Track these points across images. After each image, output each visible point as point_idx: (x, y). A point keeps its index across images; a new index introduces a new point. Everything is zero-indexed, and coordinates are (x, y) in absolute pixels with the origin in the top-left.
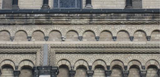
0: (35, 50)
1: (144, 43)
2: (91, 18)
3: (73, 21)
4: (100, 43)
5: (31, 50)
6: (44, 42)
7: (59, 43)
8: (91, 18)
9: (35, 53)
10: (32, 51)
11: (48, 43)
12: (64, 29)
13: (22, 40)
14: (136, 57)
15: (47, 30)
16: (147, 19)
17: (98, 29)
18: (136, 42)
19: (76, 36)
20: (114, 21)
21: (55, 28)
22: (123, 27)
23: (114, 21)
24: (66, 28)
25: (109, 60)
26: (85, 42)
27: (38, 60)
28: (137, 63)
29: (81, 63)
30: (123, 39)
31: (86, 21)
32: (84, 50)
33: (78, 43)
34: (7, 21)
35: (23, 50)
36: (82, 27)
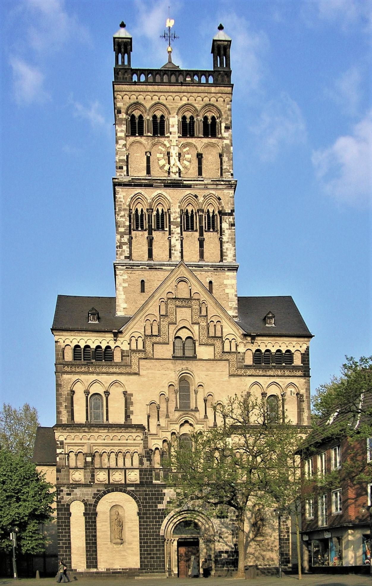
0: (83, 445)
1: (132, 442)
2: (109, 430)
3: (100, 431)
4: (113, 442)
5: (82, 445)
6: (88, 441)
7: (94, 442)
8: (109, 430)
11: (89, 441)
12: (96, 435)
13: (78, 440)
14: (128, 448)
15: (88, 435)
16: (134, 430)
17: (111, 435)
18: (129, 441)
19: (102, 438)
20: (119, 431)
21: (92, 434)
22: (123, 434)
23: (119, 431)
24: (97, 434)
25: (116, 449)
26: (106, 441)
27: (85, 450)
28: (129, 451)
29: (104, 451)
30: (123, 440)
31: (106, 431)
32: (105, 445)
33: (103, 441)
34: (70, 431)
35: (78, 445)
36: (104, 434)
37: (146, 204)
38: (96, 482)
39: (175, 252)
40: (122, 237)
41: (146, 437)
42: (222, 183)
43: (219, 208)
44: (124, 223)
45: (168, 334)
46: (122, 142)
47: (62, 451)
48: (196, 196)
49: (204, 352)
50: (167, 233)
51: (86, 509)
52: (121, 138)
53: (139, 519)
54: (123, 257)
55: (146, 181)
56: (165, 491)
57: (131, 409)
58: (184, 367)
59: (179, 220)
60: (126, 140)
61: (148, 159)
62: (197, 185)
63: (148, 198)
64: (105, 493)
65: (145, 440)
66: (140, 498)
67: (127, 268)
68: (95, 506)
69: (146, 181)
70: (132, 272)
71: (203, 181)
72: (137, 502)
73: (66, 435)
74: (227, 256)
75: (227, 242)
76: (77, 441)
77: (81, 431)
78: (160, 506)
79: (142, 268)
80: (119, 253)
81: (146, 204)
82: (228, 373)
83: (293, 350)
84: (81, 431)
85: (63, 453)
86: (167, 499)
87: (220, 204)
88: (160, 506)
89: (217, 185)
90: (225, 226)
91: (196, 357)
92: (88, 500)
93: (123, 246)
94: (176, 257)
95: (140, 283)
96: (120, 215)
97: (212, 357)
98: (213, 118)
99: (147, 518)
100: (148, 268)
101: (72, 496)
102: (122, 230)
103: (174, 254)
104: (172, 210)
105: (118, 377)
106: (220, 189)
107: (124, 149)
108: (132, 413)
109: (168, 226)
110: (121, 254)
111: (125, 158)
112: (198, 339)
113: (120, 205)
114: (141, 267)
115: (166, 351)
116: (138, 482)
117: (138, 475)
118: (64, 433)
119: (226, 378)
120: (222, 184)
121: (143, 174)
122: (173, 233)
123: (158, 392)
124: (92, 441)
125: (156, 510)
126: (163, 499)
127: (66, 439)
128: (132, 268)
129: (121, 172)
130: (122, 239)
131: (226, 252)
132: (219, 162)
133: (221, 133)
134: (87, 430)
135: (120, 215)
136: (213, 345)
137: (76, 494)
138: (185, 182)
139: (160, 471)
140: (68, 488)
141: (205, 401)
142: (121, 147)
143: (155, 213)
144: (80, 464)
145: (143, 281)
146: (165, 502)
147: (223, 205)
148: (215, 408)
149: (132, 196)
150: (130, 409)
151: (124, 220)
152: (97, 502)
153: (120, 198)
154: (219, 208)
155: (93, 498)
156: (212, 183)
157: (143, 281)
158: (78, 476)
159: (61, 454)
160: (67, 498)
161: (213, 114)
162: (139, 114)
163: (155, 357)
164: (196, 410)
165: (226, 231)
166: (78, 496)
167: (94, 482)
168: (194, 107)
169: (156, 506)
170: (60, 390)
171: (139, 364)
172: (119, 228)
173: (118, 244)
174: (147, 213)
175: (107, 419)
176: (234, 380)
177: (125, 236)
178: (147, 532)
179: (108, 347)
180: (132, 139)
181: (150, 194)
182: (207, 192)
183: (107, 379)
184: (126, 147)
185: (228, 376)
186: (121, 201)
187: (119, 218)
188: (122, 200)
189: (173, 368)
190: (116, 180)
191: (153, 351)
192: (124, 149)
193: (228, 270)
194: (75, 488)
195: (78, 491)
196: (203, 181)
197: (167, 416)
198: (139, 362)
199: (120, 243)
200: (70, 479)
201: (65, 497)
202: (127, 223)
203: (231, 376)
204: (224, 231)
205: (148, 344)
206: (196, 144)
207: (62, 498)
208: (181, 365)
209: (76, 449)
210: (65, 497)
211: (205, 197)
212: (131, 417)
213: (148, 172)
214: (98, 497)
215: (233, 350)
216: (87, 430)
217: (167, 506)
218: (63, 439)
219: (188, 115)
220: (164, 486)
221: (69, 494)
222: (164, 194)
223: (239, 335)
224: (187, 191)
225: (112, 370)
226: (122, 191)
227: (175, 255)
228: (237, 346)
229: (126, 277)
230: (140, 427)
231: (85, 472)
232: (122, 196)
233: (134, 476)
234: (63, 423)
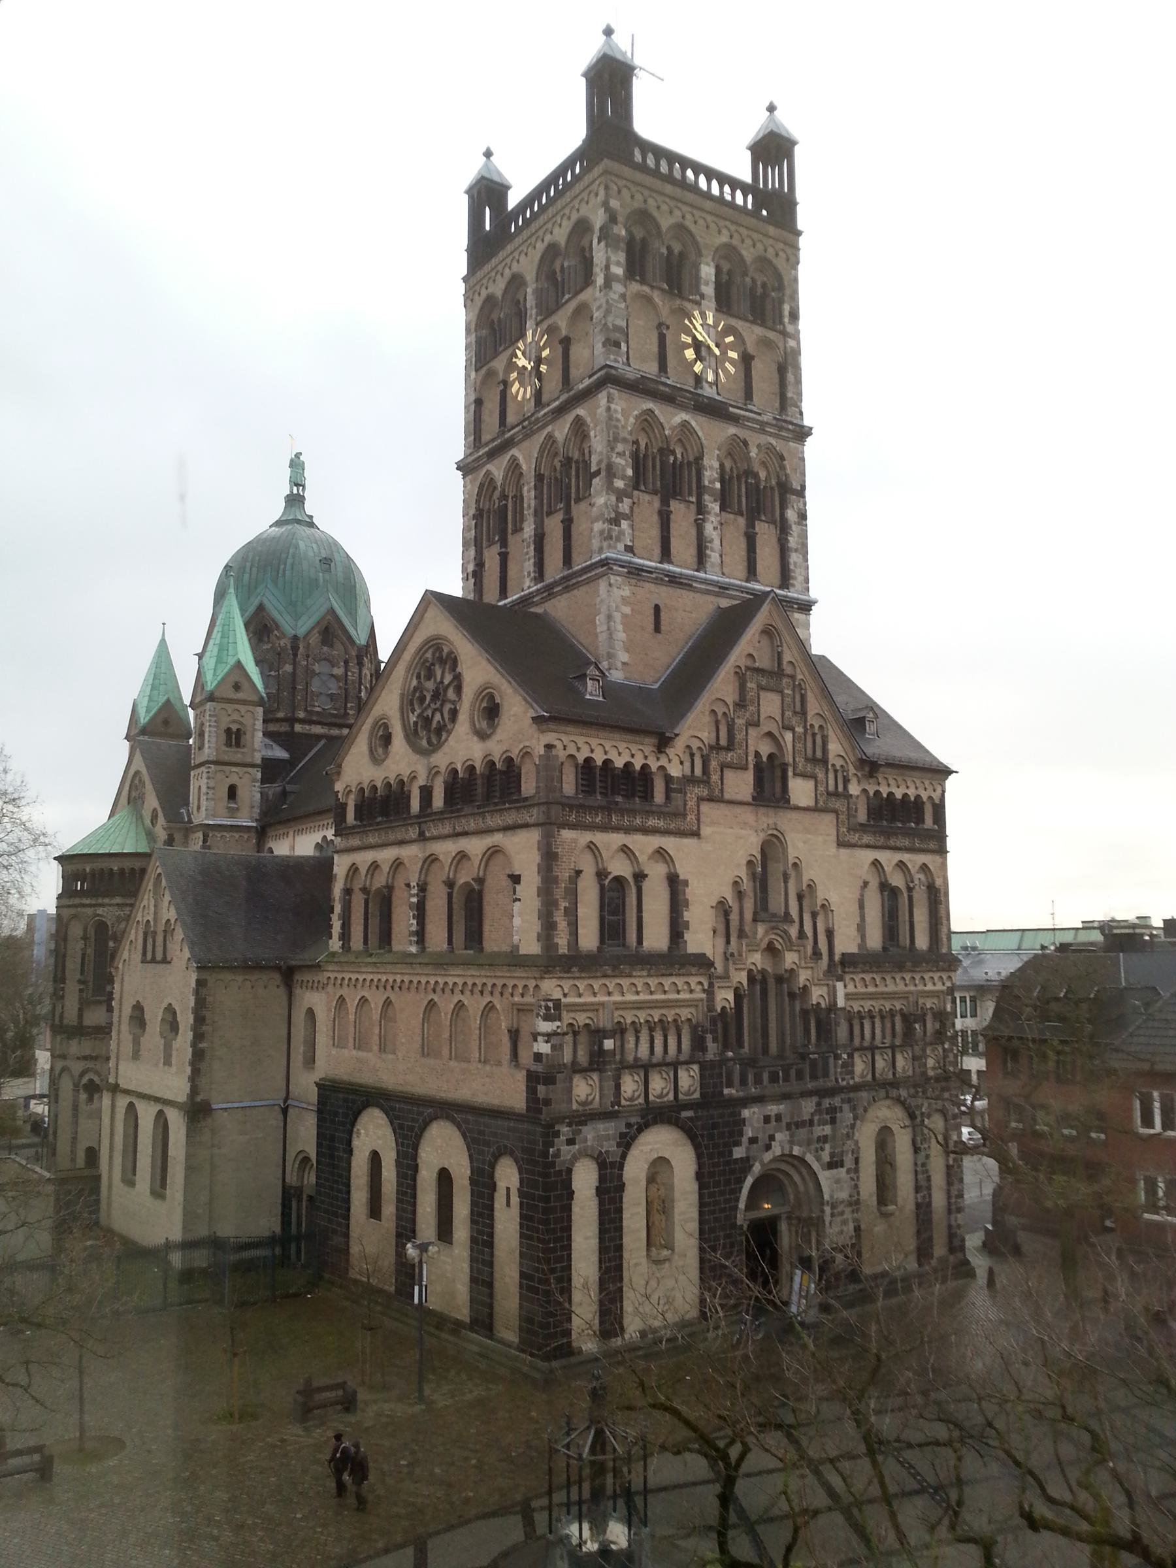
2: (649, 970)
3: (634, 974)
6: (606, 999)
9: (597, 1010)
10: (594, 1008)
16: (694, 970)
27: (604, 1021)
31: (645, 973)
37: (658, 435)
38: (623, 1102)
39: (713, 554)
40: (619, 500)
41: (711, 985)
42: (790, 427)
43: (778, 477)
44: (624, 470)
45: (747, 746)
46: (618, 288)
47: (558, 1027)
48: (745, 443)
49: (801, 791)
50: (693, 507)
51: (602, 1179)
52: (616, 278)
53: (700, 1188)
54: (621, 547)
55: (667, 389)
56: (746, 1113)
57: (687, 916)
58: (771, 822)
59: (718, 485)
60: (625, 286)
61: (662, 339)
62: (749, 419)
63: (666, 426)
64: (640, 1130)
65: (710, 992)
66: (702, 1136)
67: (629, 572)
68: (621, 1167)
69: (667, 389)
70: (639, 584)
71: (760, 414)
72: (697, 1147)
73: (567, 985)
74: (795, 578)
75: (796, 551)
76: (588, 999)
77: (598, 974)
78: (738, 1153)
79: (656, 578)
80: (614, 534)
81: (658, 435)
82: (835, 839)
83: (924, 796)
84: (598, 974)
85: (559, 1031)
86: (749, 1132)
87: (783, 468)
88: (738, 1153)
89: (781, 428)
90: (791, 515)
91: (788, 801)
92: (607, 1152)
93: (622, 521)
94: (713, 565)
95: (652, 611)
96: (617, 450)
97: (812, 803)
98: (764, 285)
99: (717, 1184)
100: (667, 579)
101: (577, 1147)
102: (619, 484)
103: (710, 557)
104: (706, 461)
105: (663, 839)
106: (784, 439)
107: (623, 306)
108: (687, 925)
109: (694, 493)
110: (618, 540)
111: (624, 324)
112: (791, 760)
113: (616, 427)
114: (654, 576)
115: (741, 785)
116: (697, 1095)
117: (697, 1078)
118: (564, 981)
119: (833, 849)
120: (789, 430)
121: (651, 368)
122: (709, 513)
123: (729, 879)
124: (617, 998)
125: (728, 1163)
126: (741, 1134)
127: (565, 995)
128: (638, 575)
129: (618, 354)
130: (620, 505)
131: (794, 572)
132: (777, 381)
133: (781, 322)
134: (609, 972)
135: (617, 450)
136: (813, 777)
137: (586, 1140)
138: (731, 409)
139: (735, 1064)
140: (570, 1125)
141: (800, 897)
142: (616, 297)
143: (672, 458)
144: (583, 1058)
145: (657, 609)
146: (745, 1140)
147: (788, 471)
148: (814, 915)
149: (636, 413)
150: (683, 917)
151: (623, 462)
152: (624, 1156)
153: (616, 411)
154: (778, 477)
155: (619, 1145)
156: (774, 422)
157: (657, 609)
158: (583, 1089)
159: (555, 1034)
160: (567, 1151)
161: (765, 279)
162: (641, 235)
163: (727, 796)
164: (787, 918)
165: (794, 527)
166: (589, 1143)
167: (619, 1104)
168: (740, 255)
169: (731, 1153)
170: (555, 869)
171: (698, 811)
172: (615, 480)
173: (613, 515)
174: (658, 457)
175: (640, 941)
176: (844, 852)
177: (625, 499)
178: (716, 1220)
179: (645, 767)
180: (635, 287)
181: (673, 418)
182: (764, 439)
183: (644, 845)
184: (625, 301)
185: (835, 845)
186: (618, 420)
187: (614, 455)
188: (619, 416)
189: (754, 824)
190: (613, 372)
191: (722, 783)
192: (623, 306)
193: (798, 609)
194: (584, 1123)
195: (591, 1133)
196: (760, 414)
197: (742, 934)
198: (698, 807)
199: (617, 513)
200: (574, 1101)
201: (565, 1148)
202: (630, 472)
203: (841, 844)
204: (790, 528)
205: (714, 764)
206: (744, 334)
207: (558, 1154)
208: (768, 819)
209: (582, 1019)
210: (565, 1148)
211: (759, 446)
212: (687, 936)
213: (663, 367)
214: (626, 1142)
215: (840, 789)
216: (609, 972)
217: (748, 1149)
218: (561, 996)
219: (726, 267)
220: (746, 1102)
221: (571, 1142)
222: (693, 423)
223: (853, 759)
224: (732, 430)
225: (652, 822)
226: (620, 398)
227: (713, 560)
228: (846, 781)
229: (626, 592)
230: (702, 962)
231: (601, 1080)
232: (619, 409)
233: (688, 1079)
234: (561, 951)
